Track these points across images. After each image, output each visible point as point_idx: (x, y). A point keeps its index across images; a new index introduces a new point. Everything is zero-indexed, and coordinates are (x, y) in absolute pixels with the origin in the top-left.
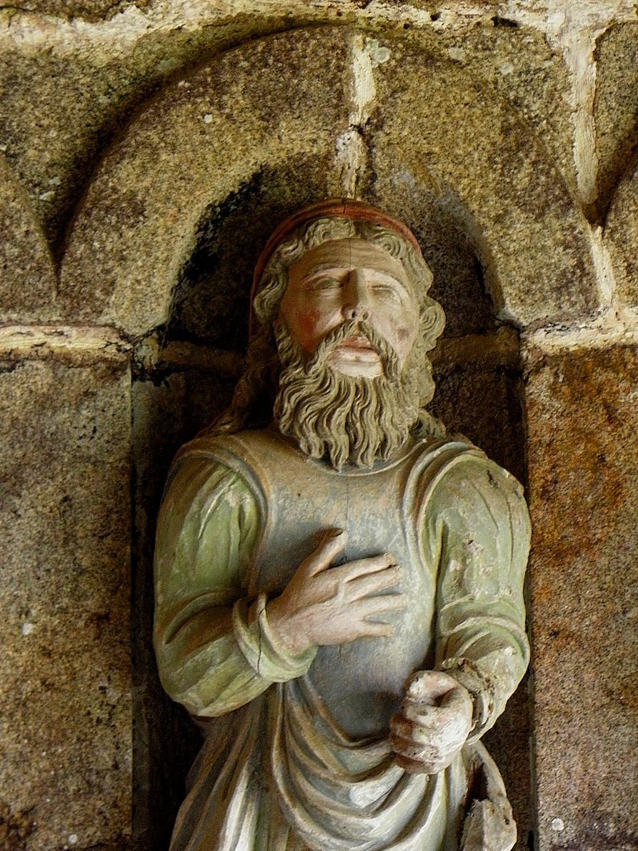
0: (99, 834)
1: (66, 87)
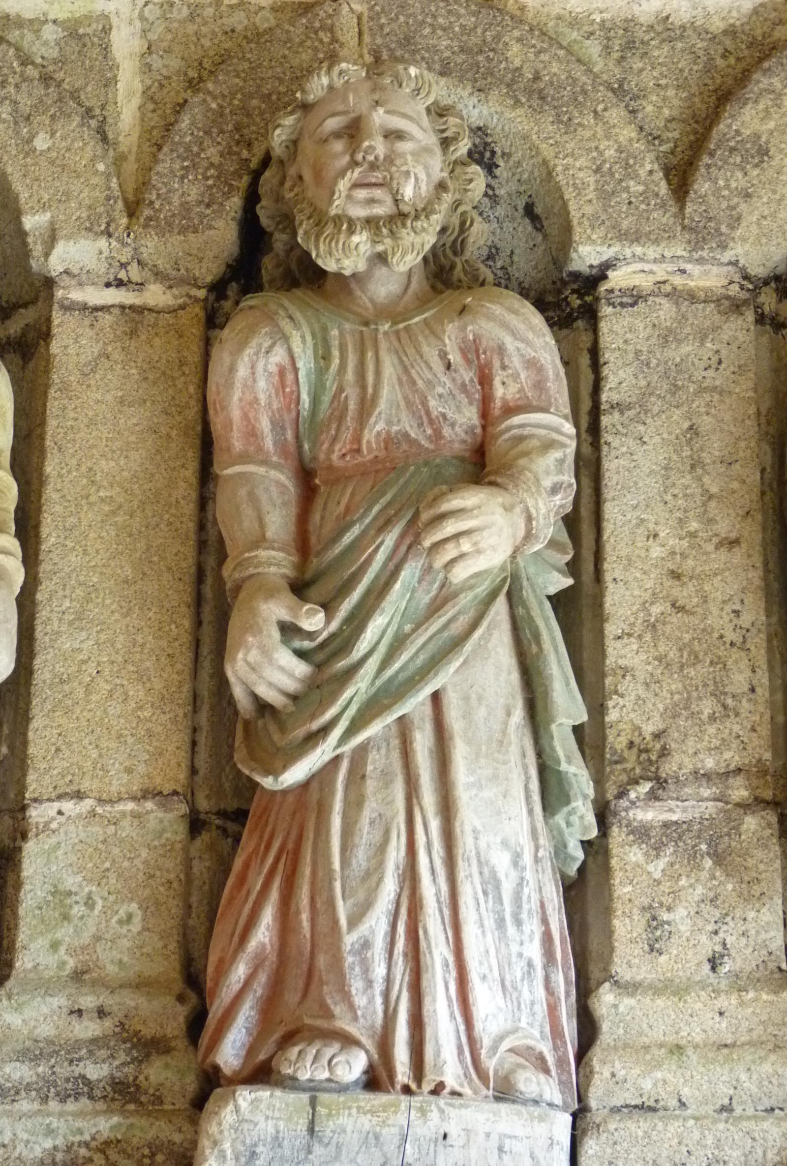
0: (737, 758)
1: (683, 51)
